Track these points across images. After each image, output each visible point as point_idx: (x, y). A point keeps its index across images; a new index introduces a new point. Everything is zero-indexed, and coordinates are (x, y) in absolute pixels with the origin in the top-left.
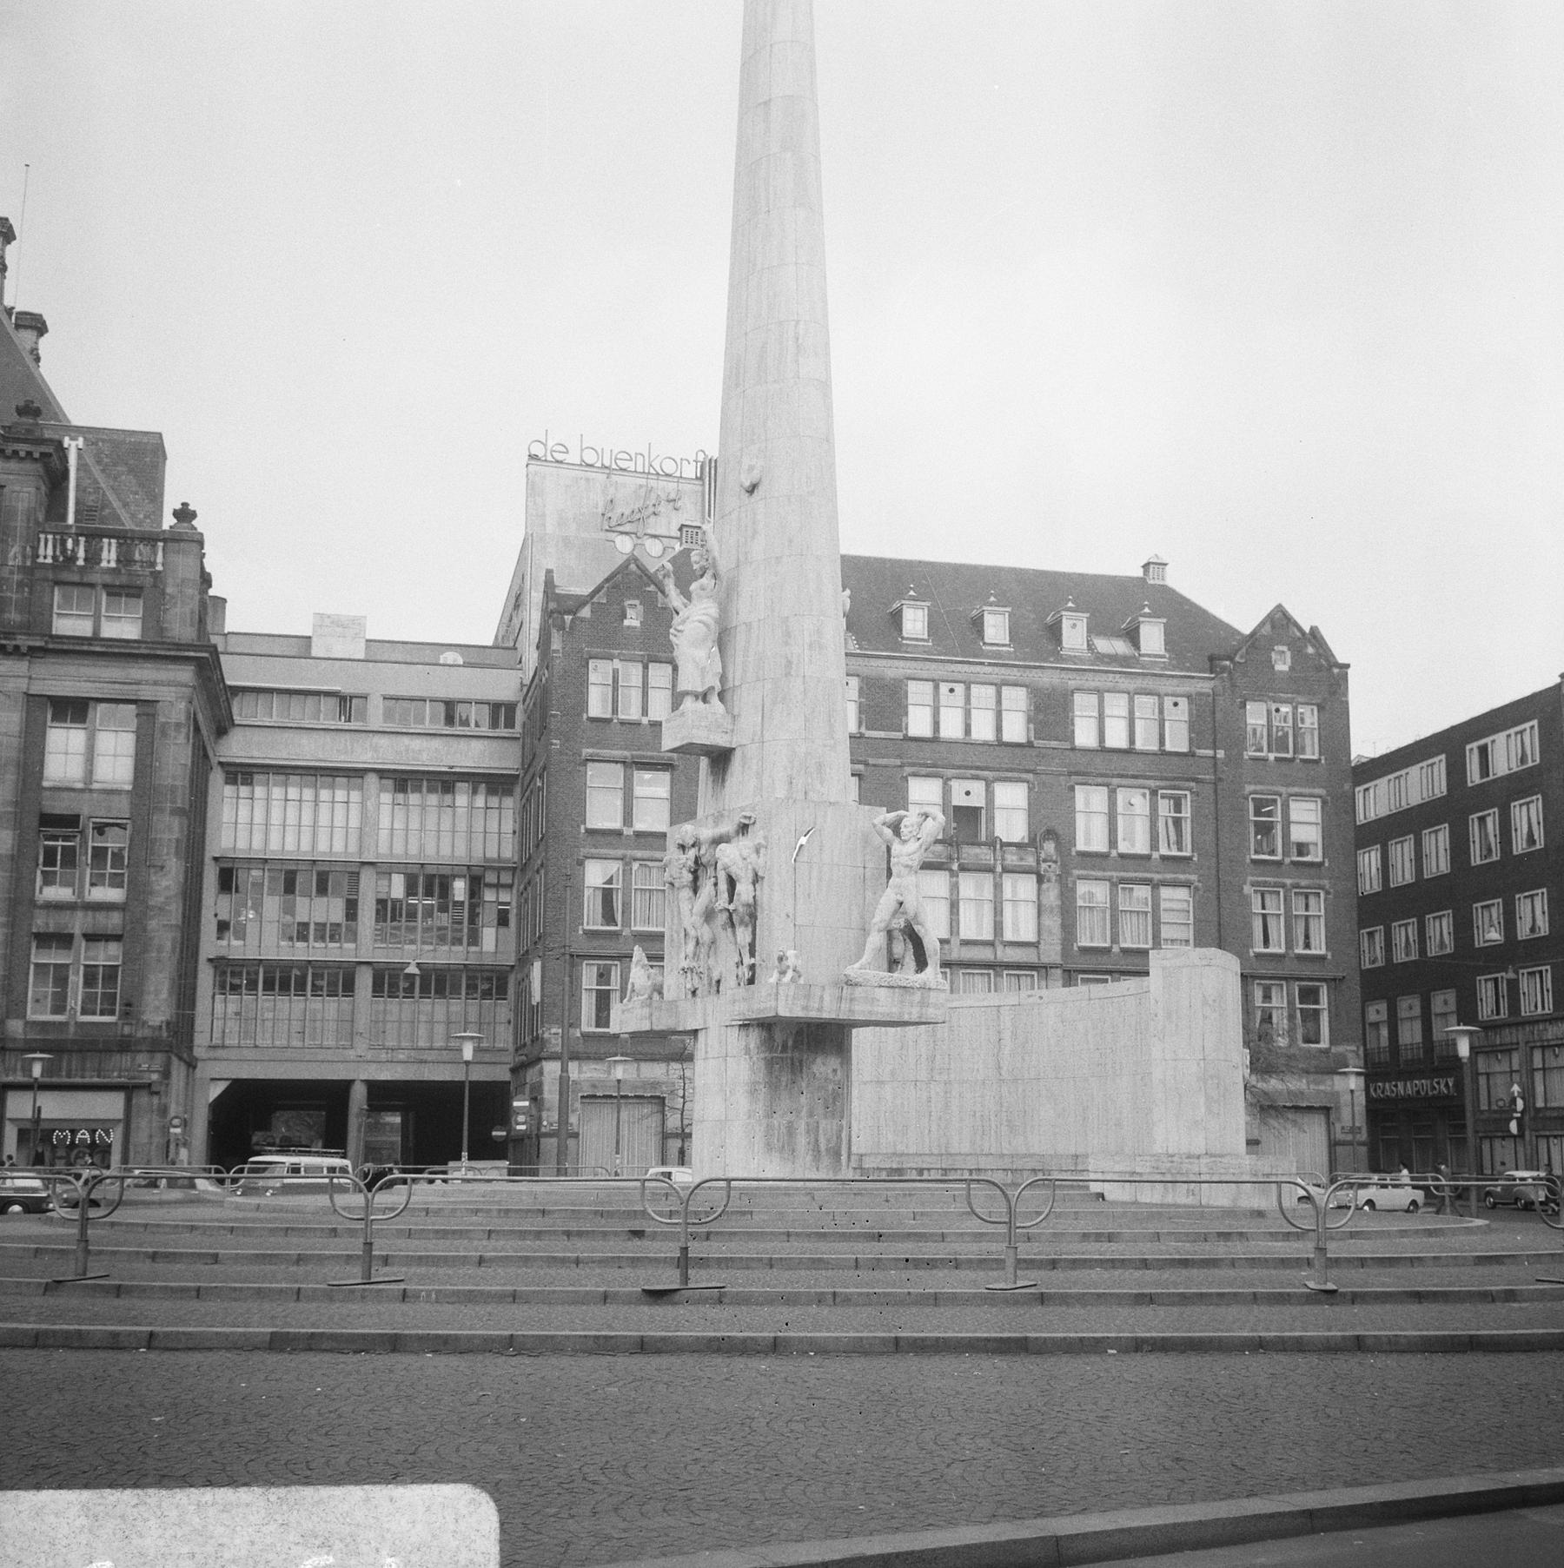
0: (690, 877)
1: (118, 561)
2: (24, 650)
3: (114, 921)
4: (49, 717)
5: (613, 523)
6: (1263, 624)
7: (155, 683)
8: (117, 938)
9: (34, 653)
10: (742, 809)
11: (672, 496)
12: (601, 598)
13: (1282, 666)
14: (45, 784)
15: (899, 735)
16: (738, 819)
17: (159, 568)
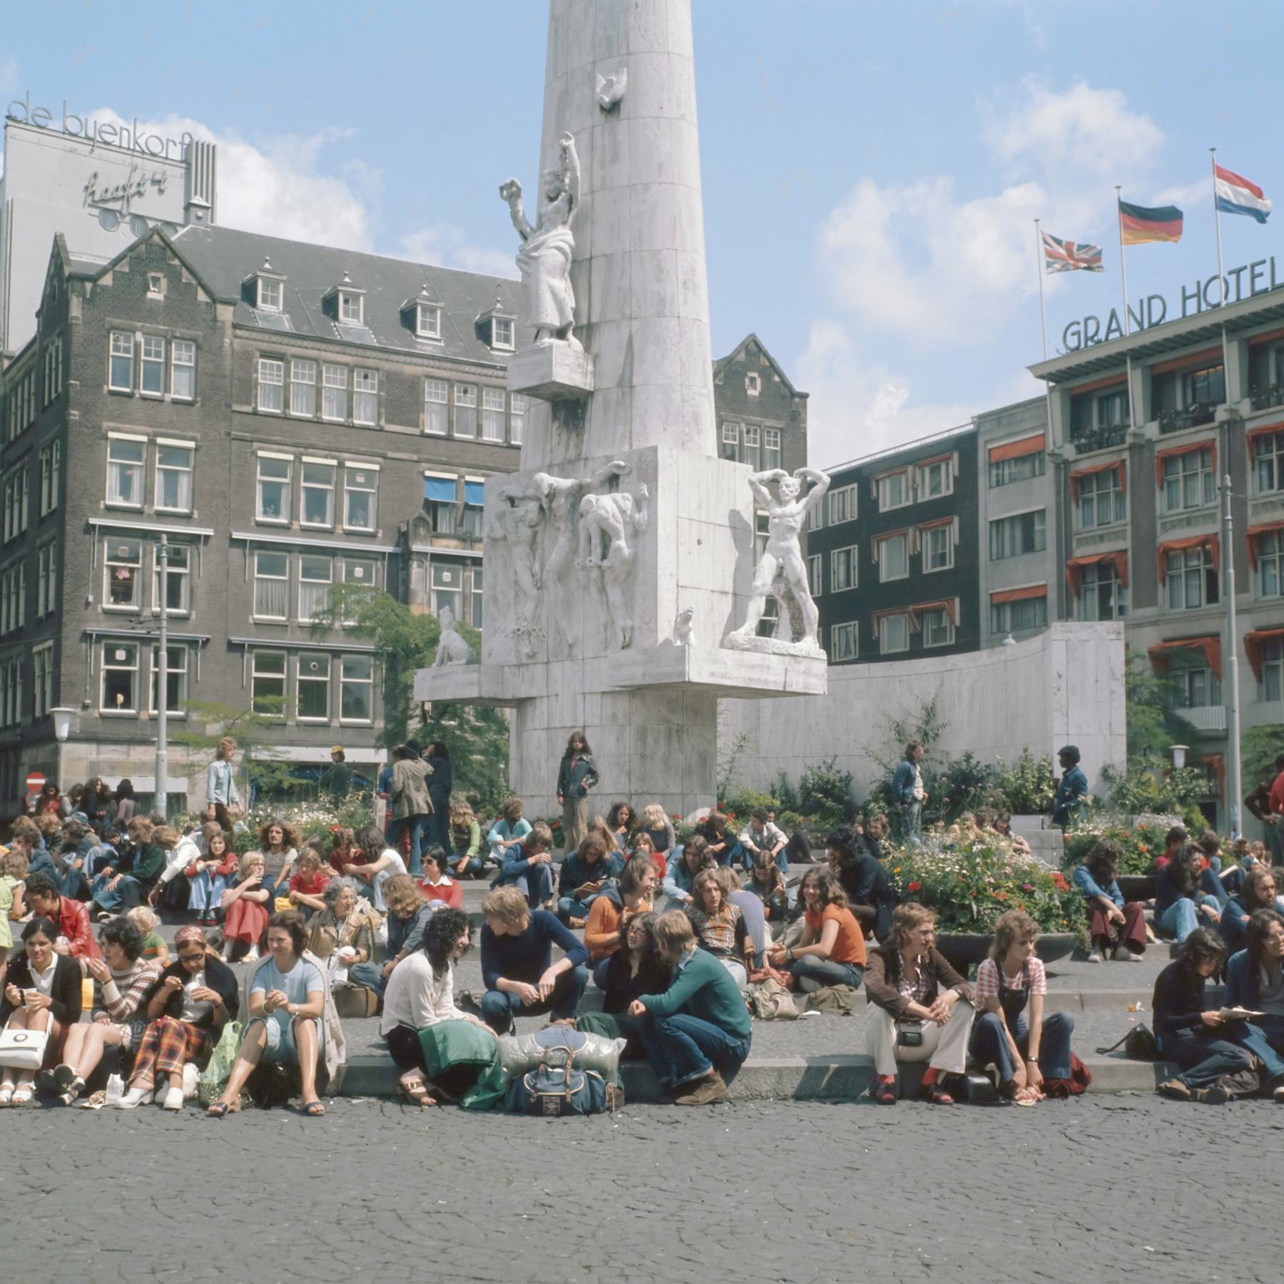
0: (529, 532)
5: (97, 197)
6: (737, 351)
10: (609, 459)
11: (158, 177)
12: (124, 268)
13: (753, 393)
15: (416, 431)
16: (604, 470)
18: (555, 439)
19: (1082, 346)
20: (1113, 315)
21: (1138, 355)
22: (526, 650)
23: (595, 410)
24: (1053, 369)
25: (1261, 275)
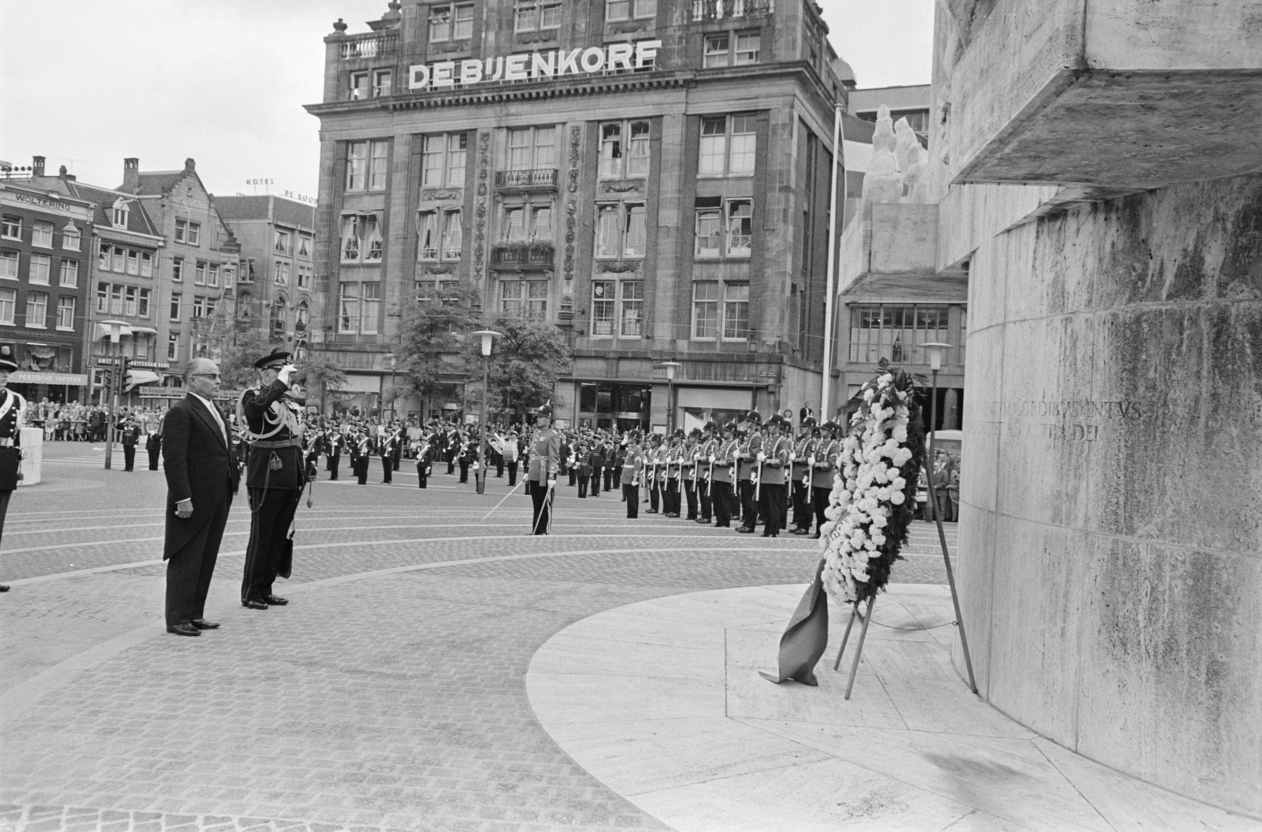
1: (745, 11)
2: (681, 82)
3: (743, 271)
4: (702, 130)
7: (768, 96)
8: (744, 283)
9: (688, 85)
14: (699, 177)
17: (771, 11)
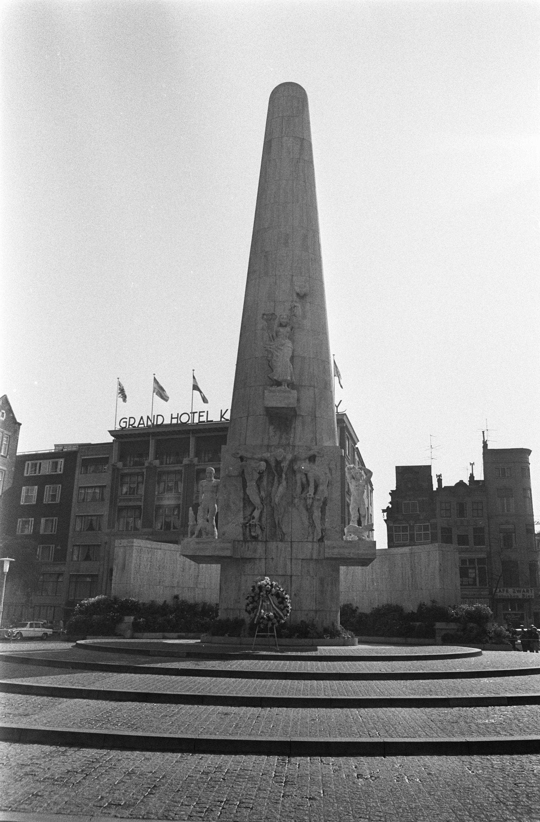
18: (272, 433)
19: (127, 427)
20: (142, 418)
21: (154, 434)
22: (253, 534)
23: (298, 424)
24: (119, 433)
25: (203, 416)
